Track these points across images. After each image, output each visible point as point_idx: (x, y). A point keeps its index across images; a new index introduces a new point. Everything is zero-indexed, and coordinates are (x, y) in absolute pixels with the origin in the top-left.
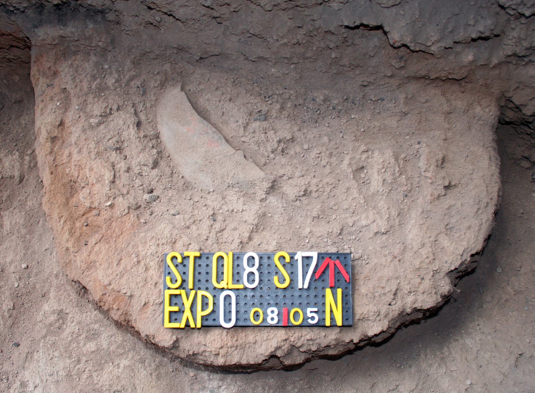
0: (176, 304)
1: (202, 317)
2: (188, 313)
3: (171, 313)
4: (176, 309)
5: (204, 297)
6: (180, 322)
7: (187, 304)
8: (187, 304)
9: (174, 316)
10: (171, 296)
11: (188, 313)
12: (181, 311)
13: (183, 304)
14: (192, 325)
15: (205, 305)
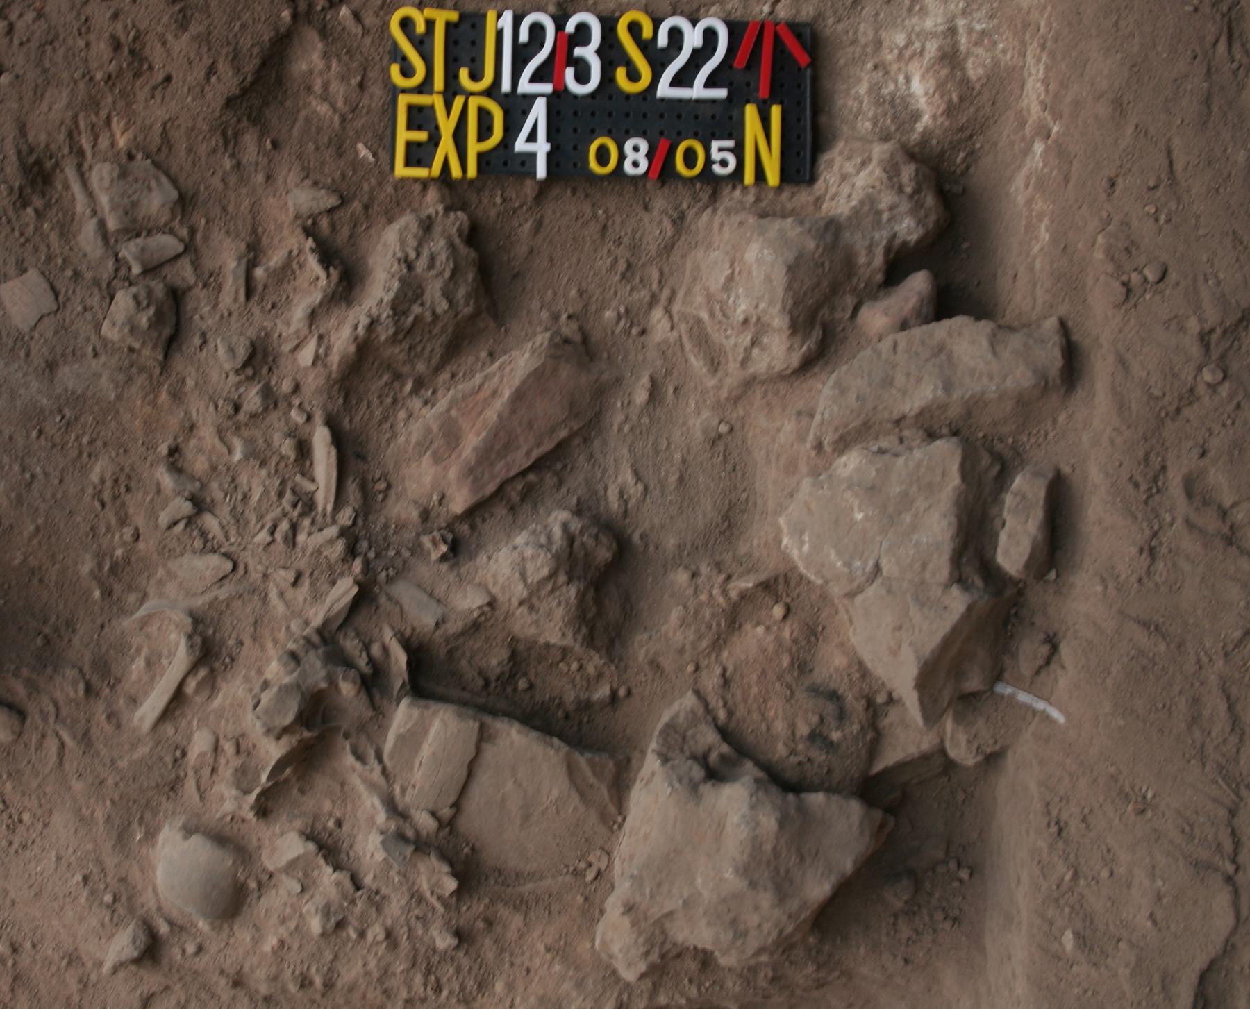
0: (419, 128)
1: (481, 156)
2: (447, 146)
3: (409, 145)
4: (422, 136)
5: (484, 115)
6: (429, 166)
7: (447, 126)
8: (447, 126)
9: (417, 154)
10: (411, 109)
11: (447, 146)
12: (435, 140)
13: (437, 128)
14: (456, 172)
15: (485, 131)
